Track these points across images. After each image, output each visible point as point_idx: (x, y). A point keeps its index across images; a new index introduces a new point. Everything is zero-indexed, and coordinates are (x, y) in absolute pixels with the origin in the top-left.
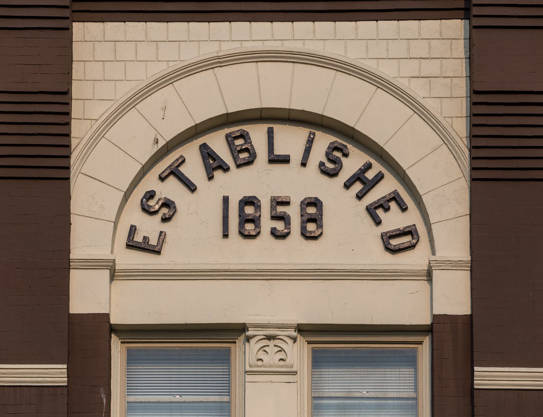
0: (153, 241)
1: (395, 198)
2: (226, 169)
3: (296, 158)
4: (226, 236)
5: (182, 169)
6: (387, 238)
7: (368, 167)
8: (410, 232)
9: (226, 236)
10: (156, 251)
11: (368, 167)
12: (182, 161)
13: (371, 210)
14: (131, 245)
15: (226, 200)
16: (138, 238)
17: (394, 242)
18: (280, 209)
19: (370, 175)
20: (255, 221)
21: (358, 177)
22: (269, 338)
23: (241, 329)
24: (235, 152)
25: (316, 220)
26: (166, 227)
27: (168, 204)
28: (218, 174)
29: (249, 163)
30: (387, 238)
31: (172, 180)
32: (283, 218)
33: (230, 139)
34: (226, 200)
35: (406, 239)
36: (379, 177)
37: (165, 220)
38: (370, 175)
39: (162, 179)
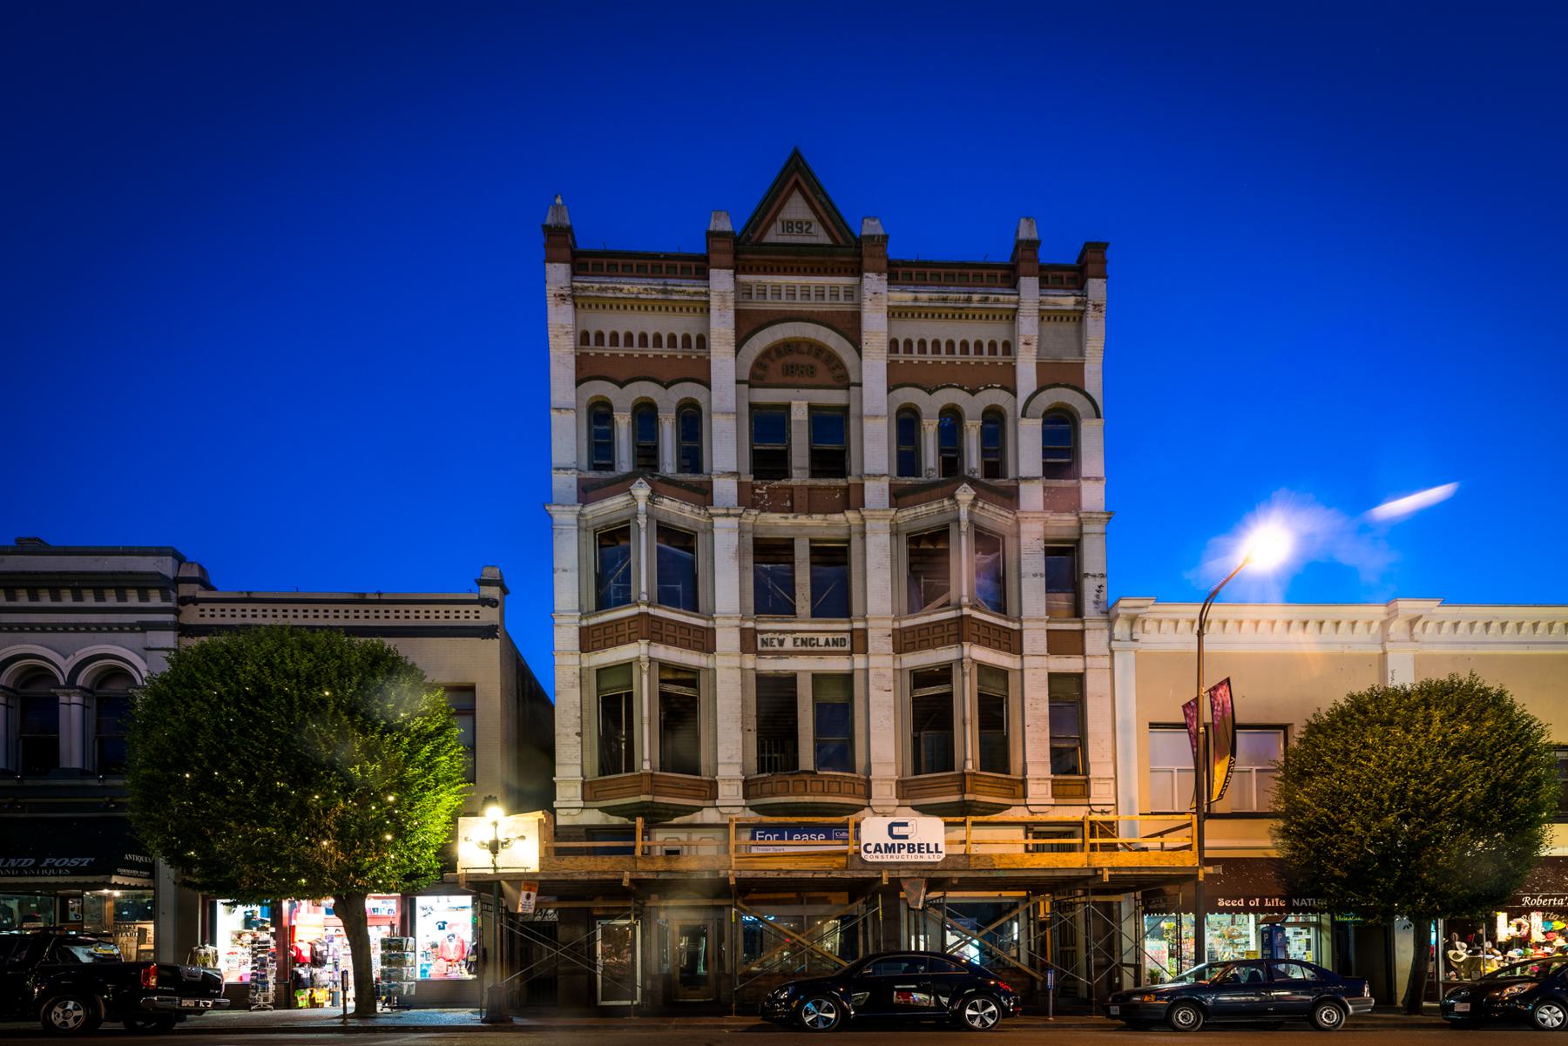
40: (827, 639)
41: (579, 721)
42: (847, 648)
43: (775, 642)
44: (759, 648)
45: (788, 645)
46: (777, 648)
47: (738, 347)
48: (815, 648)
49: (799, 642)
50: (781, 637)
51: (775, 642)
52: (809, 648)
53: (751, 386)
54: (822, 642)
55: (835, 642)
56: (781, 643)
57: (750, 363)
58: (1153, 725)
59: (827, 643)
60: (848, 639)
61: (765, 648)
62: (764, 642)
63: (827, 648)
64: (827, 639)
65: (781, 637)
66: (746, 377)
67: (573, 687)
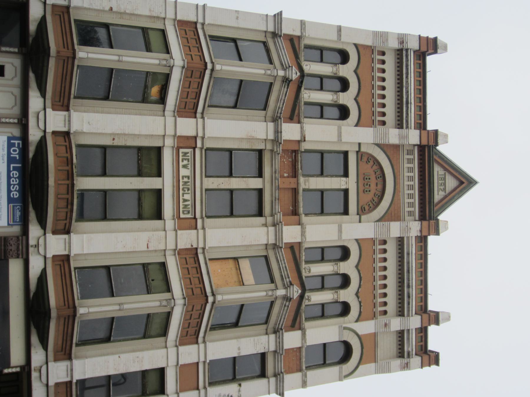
22: (346, 182)
41: (122, 11)
42: (182, 216)
43: (185, 162)
44: (181, 150)
45: (184, 172)
46: (181, 164)
47: (378, 145)
49: (186, 180)
50: (189, 166)
51: (185, 162)
52: (181, 187)
53: (357, 152)
56: (185, 166)
57: (370, 152)
59: (185, 200)
60: (189, 216)
61: (181, 154)
63: (181, 201)
64: (189, 201)
65: (189, 166)
66: (363, 149)
67: (150, 10)
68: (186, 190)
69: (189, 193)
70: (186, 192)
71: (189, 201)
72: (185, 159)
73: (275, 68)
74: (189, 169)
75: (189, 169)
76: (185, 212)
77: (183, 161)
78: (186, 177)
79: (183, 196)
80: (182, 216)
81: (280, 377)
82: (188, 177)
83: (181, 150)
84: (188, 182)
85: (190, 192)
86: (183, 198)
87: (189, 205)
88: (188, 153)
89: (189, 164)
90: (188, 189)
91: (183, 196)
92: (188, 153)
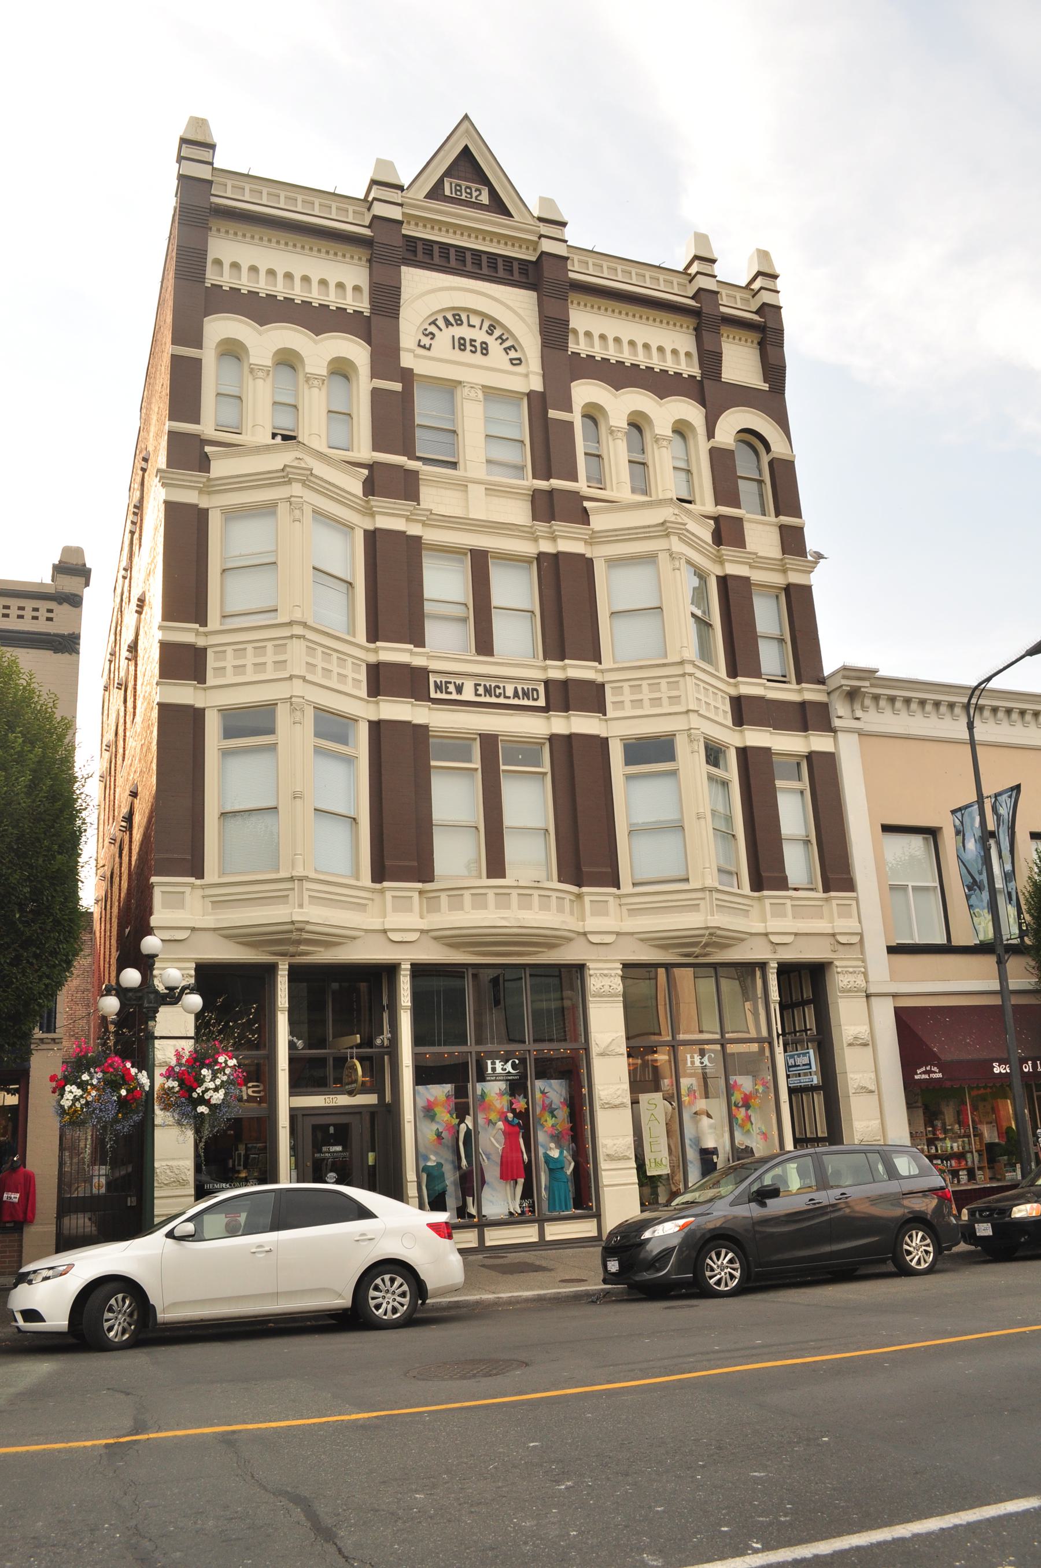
0: (427, 346)
1: (513, 347)
2: (452, 325)
3: (478, 326)
4: (454, 348)
5: (437, 322)
6: (511, 360)
7: (503, 334)
8: (519, 359)
9: (454, 348)
10: (429, 349)
11: (503, 334)
12: (437, 319)
13: (505, 349)
14: (419, 345)
15: (453, 336)
16: (422, 344)
17: (514, 362)
18: (473, 343)
19: (504, 337)
20: (464, 345)
21: (500, 337)
23: (460, 382)
24: (456, 320)
25: (486, 349)
26: (431, 342)
27: (431, 333)
28: (450, 327)
29: (461, 324)
30: (511, 360)
31: (433, 326)
32: (475, 346)
33: (454, 315)
34: (453, 336)
35: (518, 362)
36: (507, 339)
37: (432, 339)
38: (504, 337)
39: (430, 324)
40: (516, 689)
42: (541, 702)
43: (452, 688)
44: (433, 695)
45: (468, 695)
46: (455, 696)
48: (502, 700)
49: (481, 690)
52: (494, 700)
54: (510, 692)
55: (526, 694)
56: (459, 689)
58: (887, 829)
59: (516, 695)
61: (439, 696)
62: (438, 687)
63: (516, 702)
64: (516, 688)
68: (498, 691)
69: (504, 687)
70: (501, 691)
71: (516, 688)
72: (447, 688)
73: (288, 500)
74: (463, 684)
75: (463, 684)
76: (535, 697)
77: (451, 693)
78: (476, 690)
79: (509, 698)
80: (541, 702)
81: (790, 564)
82: (476, 685)
83: (433, 695)
84: (485, 686)
85: (501, 685)
86: (512, 696)
87: (523, 689)
88: (435, 682)
89: (455, 683)
90: (499, 687)
91: (509, 698)
92: (435, 682)
